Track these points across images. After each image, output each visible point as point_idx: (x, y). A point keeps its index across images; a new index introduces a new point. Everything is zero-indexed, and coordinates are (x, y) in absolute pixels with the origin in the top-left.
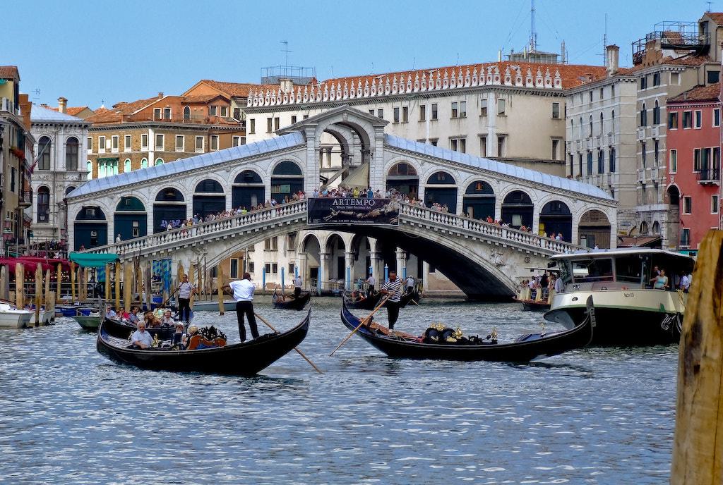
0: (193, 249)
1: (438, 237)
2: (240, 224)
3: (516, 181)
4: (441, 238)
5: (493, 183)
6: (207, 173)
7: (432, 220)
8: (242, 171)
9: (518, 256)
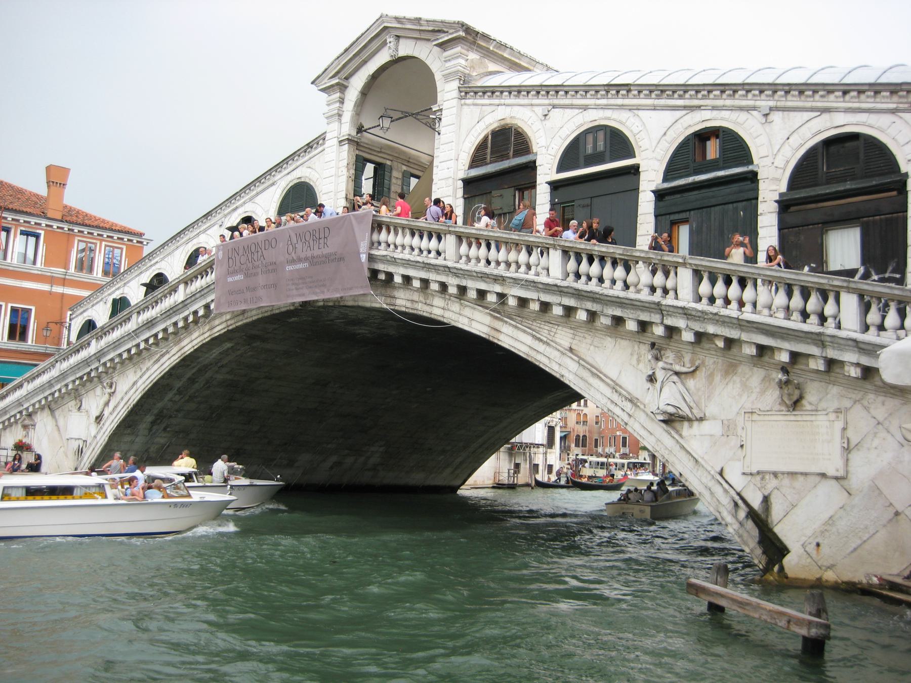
1: (487, 320)
3: (833, 101)
4: (498, 324)
5: (747, 126)
6: (198, 234)
7: (462, 265)
9: (756, 376)
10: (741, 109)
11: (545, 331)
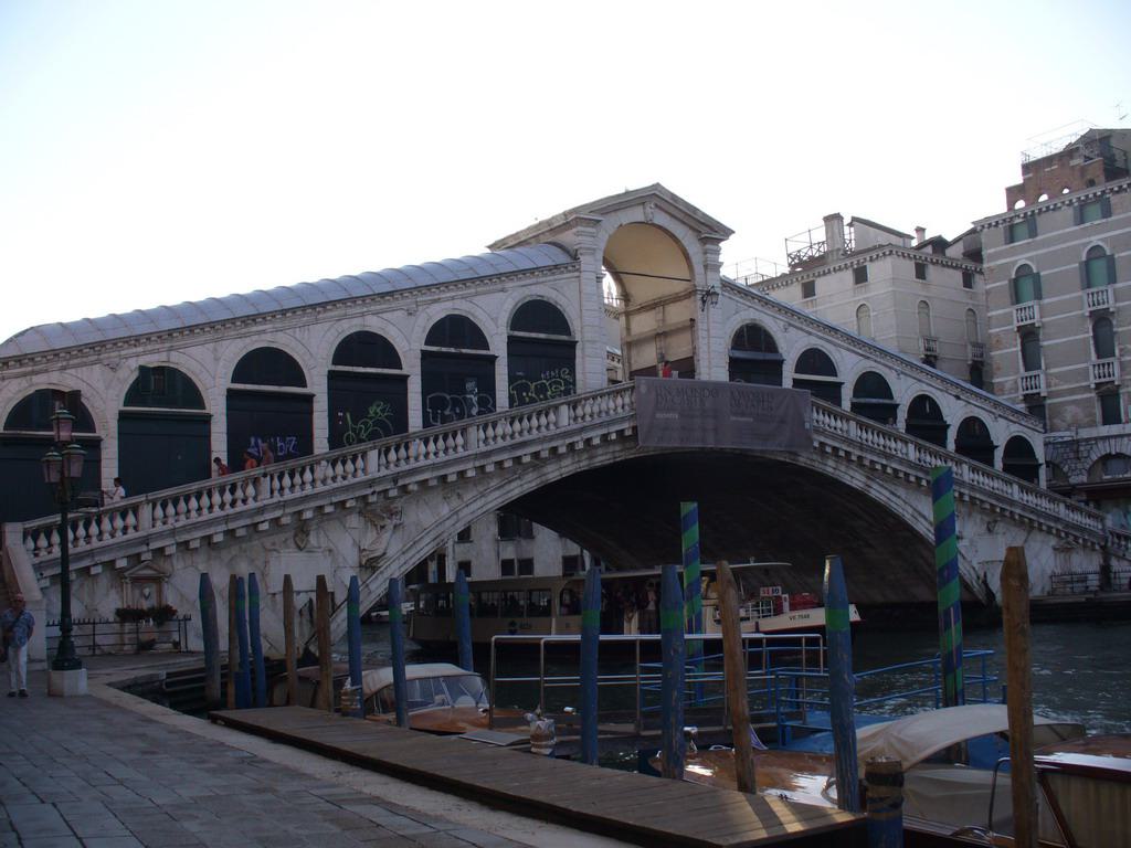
0: (365, 508)
1: (864, 479)
2: (486, 441)
4: (869, 482)
8: (443, 315)
9: (978, 517)
10: (886, 366)
11: (892, 488)
